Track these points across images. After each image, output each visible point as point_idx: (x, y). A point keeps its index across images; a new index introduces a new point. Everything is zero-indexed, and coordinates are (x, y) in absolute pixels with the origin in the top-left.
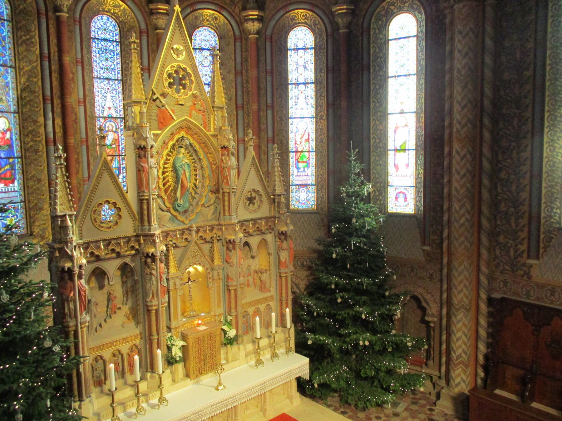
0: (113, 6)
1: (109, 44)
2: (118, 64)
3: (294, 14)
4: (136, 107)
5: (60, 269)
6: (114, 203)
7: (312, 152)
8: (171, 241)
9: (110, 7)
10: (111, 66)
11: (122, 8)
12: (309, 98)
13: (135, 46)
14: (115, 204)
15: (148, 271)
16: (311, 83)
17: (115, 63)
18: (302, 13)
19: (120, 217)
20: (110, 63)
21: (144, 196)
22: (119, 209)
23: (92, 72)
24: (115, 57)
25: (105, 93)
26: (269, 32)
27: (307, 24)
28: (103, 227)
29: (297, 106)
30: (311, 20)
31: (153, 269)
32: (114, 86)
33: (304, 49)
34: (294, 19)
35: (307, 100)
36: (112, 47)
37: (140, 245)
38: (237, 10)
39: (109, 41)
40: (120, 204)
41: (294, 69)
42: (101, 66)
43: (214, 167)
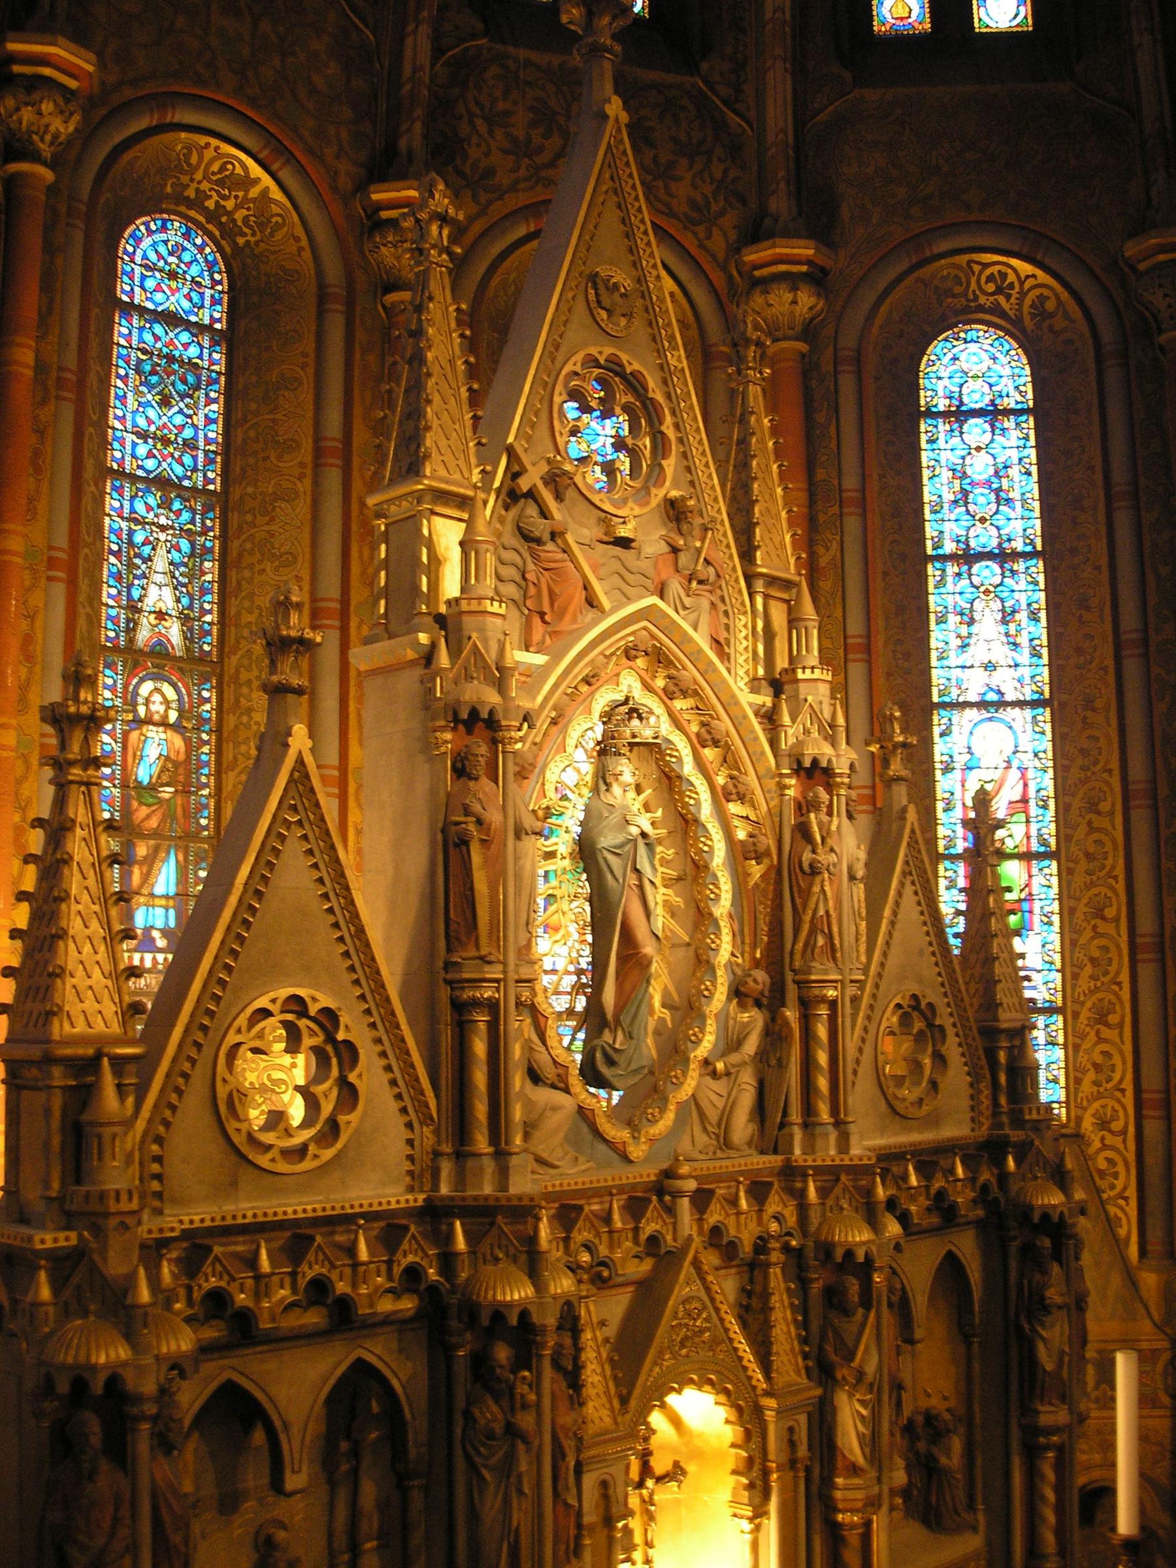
0: (221, 183)
1: (185, 337)
2: (209, 421)
3: (954, 272)
4: (438, 521)
5: (63, 1387)
6: (326, 1011)
7: (1040, 856)
8: (587, 1247)
9: (205, 186)
10: (181, 428)
11: (254, 192)
12: (1022, 616)
13: (445, 232)
14: (329, 1019)
15: (490, 1413)
16: (1025, 556)
17: (200, 421)
18: (986, 266)
19: (349, 1094)
20: (179, 420)
21: (477, 982)
22: (349, 1053)
23: (105, 444)
24: (201, 394)
25: (146, 542)
26: (849, 340)
27: (1003, 315)
28: (269, 1147)
29: (970, 650)
30: (1023, 294)
31: (525, 1407)
32: (186, 516)
33: (994, 413)
34: (949, 293)
35: (1012, 628)
36: (193, 351)
37: (447, 1261)
38: (718, 244)
39: (187, 325)
40: (352, 1028)
41: (948, 497)
42: (142, 422)
43: (756, 870)
